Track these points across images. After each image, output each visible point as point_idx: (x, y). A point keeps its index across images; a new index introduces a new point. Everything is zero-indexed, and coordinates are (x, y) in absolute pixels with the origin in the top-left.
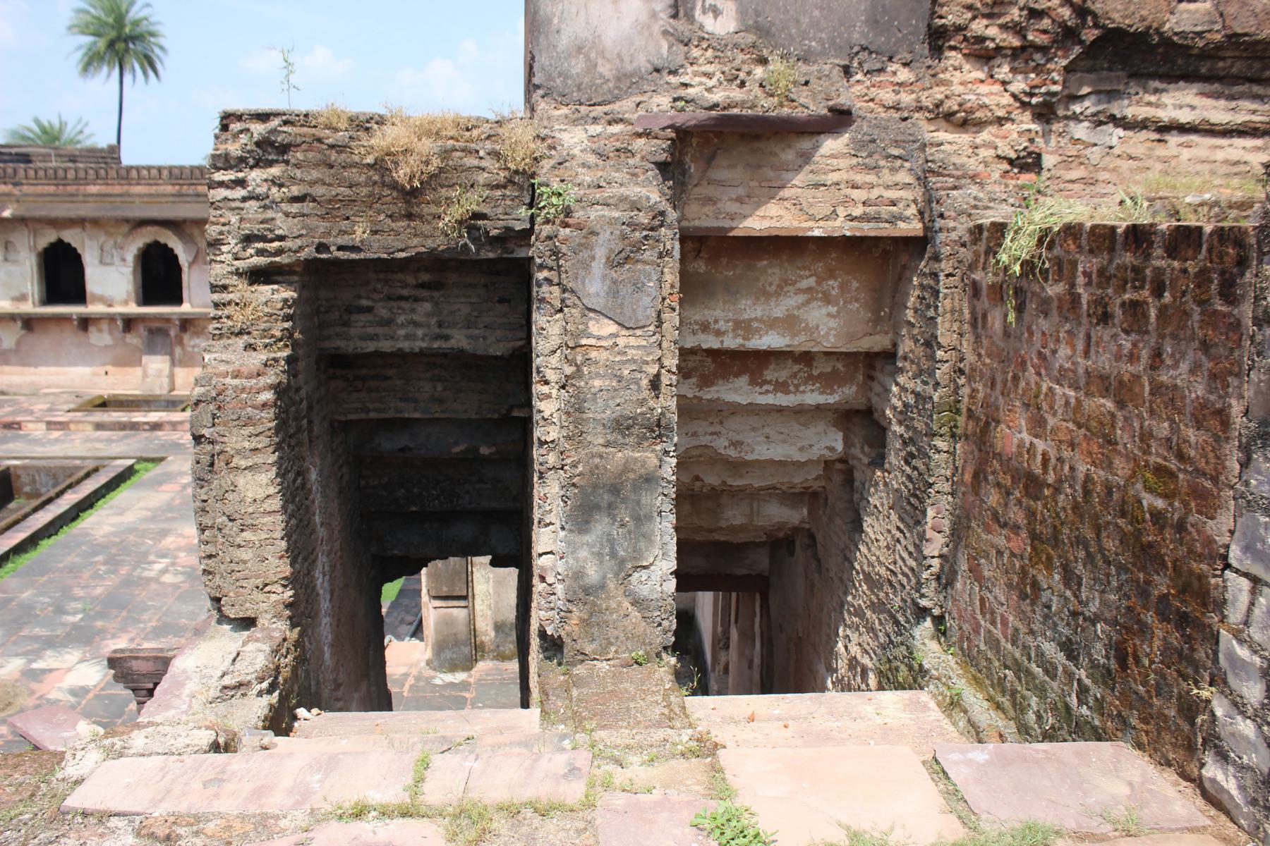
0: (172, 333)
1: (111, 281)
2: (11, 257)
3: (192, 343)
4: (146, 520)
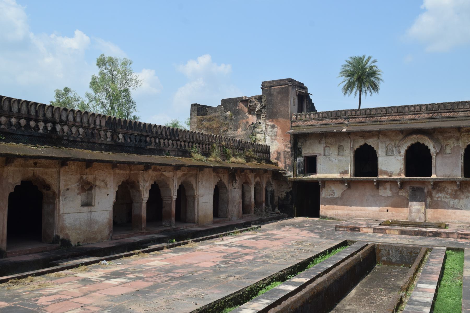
0: (426, 190)
1: (391, 164)
2: (341, 153)
3: (437, 196)
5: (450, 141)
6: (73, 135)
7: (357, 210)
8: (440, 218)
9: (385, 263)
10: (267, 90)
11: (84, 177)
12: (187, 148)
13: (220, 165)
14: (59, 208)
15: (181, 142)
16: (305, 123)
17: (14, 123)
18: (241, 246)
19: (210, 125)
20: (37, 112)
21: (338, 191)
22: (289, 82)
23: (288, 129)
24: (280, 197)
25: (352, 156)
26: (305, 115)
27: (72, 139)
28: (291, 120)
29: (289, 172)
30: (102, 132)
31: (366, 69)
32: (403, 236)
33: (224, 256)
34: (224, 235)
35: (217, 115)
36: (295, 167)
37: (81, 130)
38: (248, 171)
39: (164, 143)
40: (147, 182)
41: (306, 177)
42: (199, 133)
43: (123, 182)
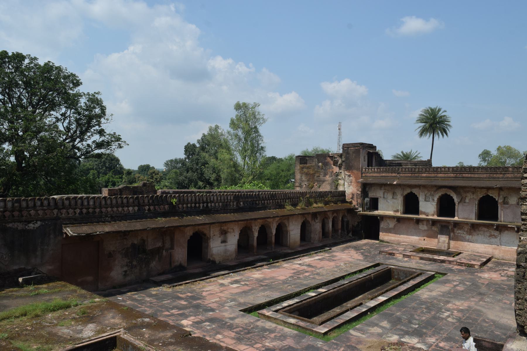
0: (450, 228)
1: (428, 208)
4: (440, 296)
12: (282, 203)
20: (199, 199)
34: (303, 256)
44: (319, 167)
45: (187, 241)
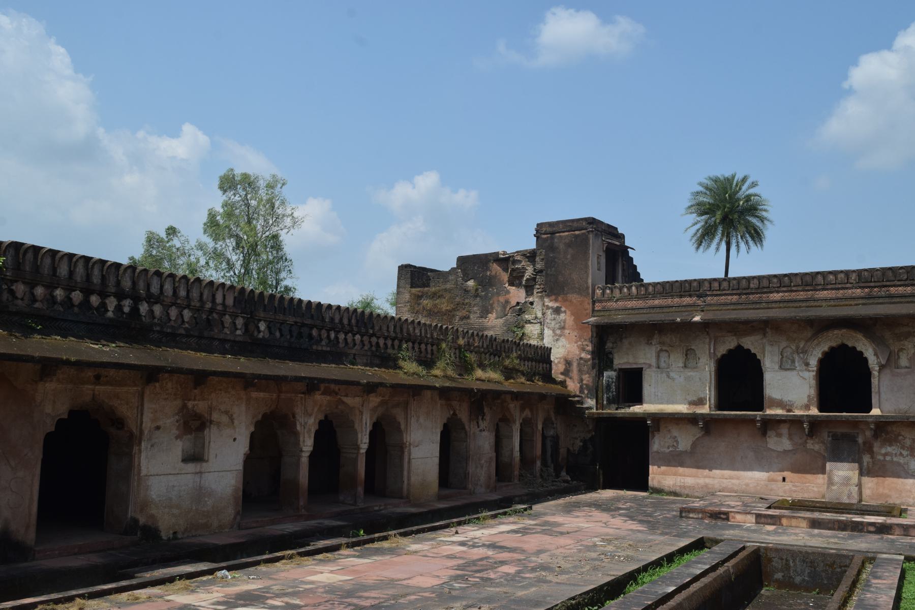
0: (860, 440)
1: (791, 387)
3: (883, 451)
5: (906, 343)
6: (172, 323)
7: (723, 477)
8: (890, 496)
9: (781, 584)
10: (546, 240)
11: (190, 404)
12: (390, 351)
13: (454, 385)
14: (139, 465)
15: (378, 338)
16: (620, 303)
17: (59, 298)
18: (493, 546)
19: (435, 306)
20: (103, 278)
21: (685, 439)
22: (590, 223)
23: (587, 316)
24: (571, 449)
25: (713, 369)
26: (621, 289)
27: (169, 330)
28: (593, 298)
29: (589, 400)
30: (227, 317)
31: (739, 200)
32: (816, 531)
33: (458, 566)
34: (459, 524)
35: (448, 286)
36: (600, 390)
37: (187, 314)
38: (508, 397)
39: (346, 339)
40: (310, 415)
41: (623, 411)
42: (413, 322)
43: (265, 416)
44: (466, 291)
45: (40, 437)
